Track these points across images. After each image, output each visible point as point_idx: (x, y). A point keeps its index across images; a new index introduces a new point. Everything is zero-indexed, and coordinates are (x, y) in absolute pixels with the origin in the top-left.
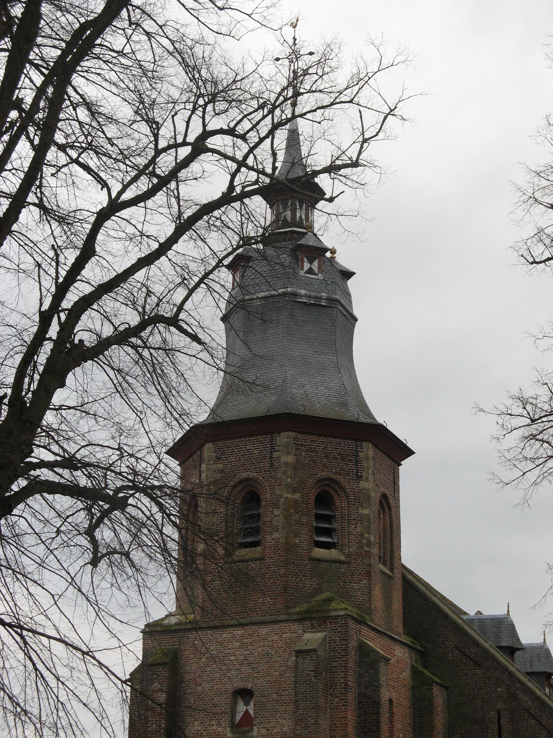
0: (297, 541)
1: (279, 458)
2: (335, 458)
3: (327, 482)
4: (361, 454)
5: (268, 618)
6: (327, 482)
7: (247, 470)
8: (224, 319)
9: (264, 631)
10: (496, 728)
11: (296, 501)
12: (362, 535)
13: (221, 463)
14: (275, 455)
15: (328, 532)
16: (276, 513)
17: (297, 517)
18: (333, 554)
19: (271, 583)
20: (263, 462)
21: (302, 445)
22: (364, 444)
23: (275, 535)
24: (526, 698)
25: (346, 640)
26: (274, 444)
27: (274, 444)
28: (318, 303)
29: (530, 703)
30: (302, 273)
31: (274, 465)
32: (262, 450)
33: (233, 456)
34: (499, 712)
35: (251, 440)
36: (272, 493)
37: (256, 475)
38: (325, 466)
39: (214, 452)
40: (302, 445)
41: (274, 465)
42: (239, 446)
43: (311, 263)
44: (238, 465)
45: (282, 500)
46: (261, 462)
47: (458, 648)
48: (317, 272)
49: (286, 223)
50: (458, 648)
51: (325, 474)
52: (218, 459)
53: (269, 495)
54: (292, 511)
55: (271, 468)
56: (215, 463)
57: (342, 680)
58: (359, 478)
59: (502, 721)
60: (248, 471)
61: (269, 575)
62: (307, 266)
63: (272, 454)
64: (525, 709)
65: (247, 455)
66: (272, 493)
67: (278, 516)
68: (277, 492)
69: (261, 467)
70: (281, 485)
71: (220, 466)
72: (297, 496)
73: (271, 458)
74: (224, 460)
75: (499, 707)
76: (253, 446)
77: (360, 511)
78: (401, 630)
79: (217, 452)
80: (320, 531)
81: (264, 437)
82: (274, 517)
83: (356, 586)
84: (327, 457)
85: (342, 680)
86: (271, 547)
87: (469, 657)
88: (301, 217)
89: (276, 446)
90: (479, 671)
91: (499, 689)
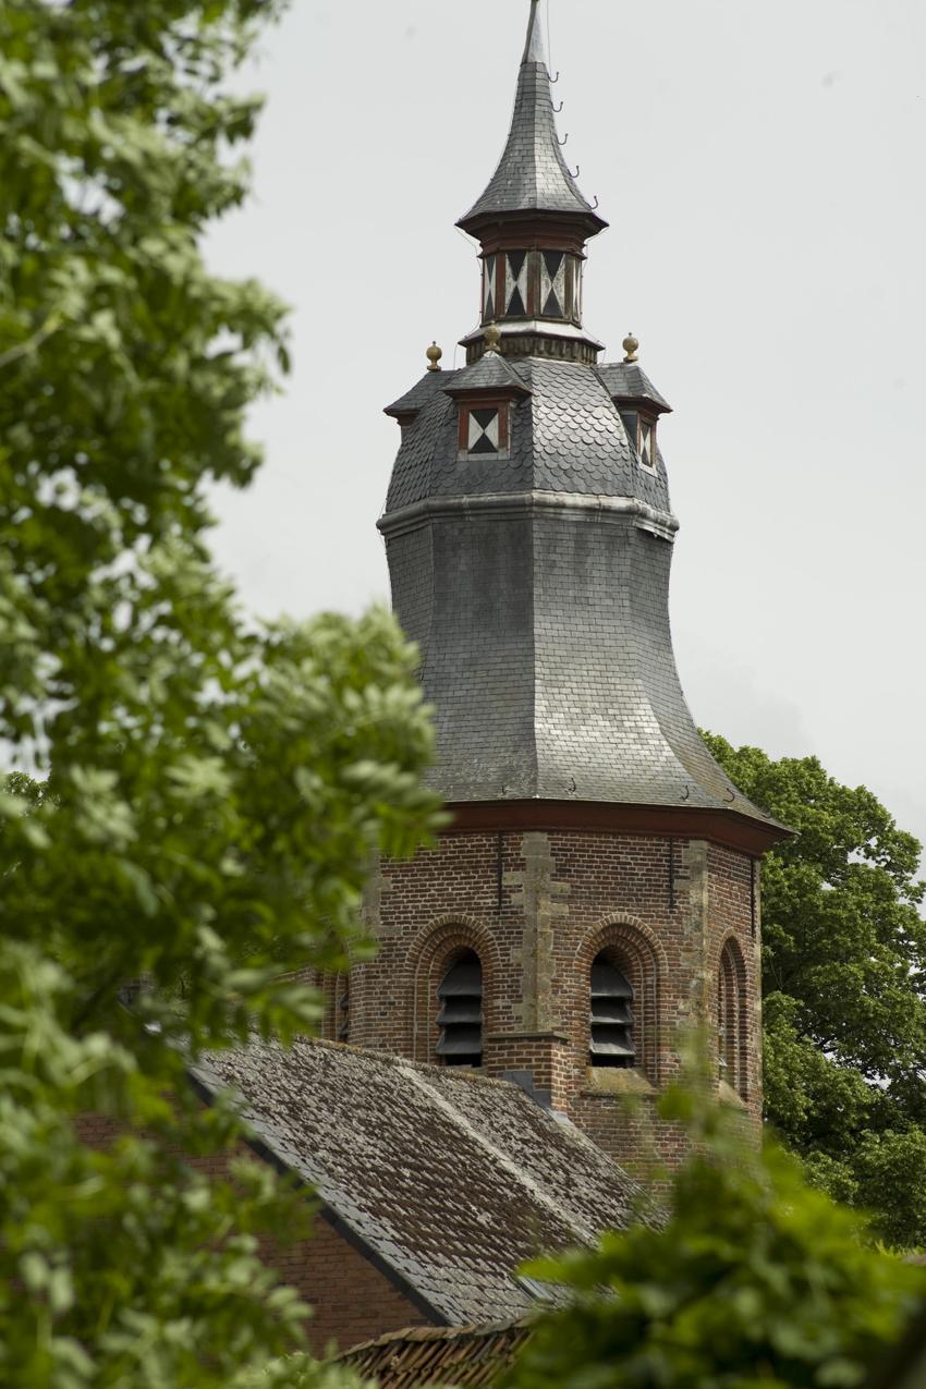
13: (568, 881)
16: (681, 1007)
19: (676, 1150)
20: (655, 896)
26: (676, 861)
27: (676, 861)
31: (676, 907)
32: (651, 870)
33: (593, 872)
35: (629, 843)
36: (674, 965)
37: (640, 920)
39: (553, 855)
41: (676, 907)
42: (605, 852)
44: (602, 893)
45: (694, 982)
46: (650, 895)
49: (516, 312)
53: (667, 967)
55: (671, 912)
56: (554, 877)
60: (623, 910)
61: (671, 1134)
63: (671, 881)
65: (620, 874)
66: (674, 965)
67: (687, 1014)
68: (685, 965)
69: (650, 906)
70: (690, 951)
71: (567, 886)
74: (573, 876)
79: (557, 855)
81: (655, 842)
86: (673, 1077)
88: (516, 291)
89: (680, 867)
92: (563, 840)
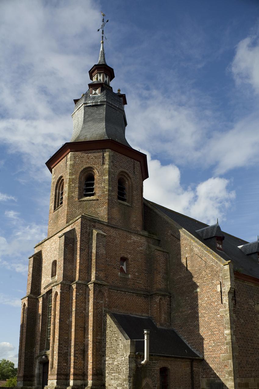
0: (73, 195)
2: (92, 158)
6: (89, 169)
11: (73, 179)
12: (104, 187)
17: (73, 185)
18: (92, 198)
22: (107, 150)
24: (196, 249)
28: (96, 104)
29: (198, 251)
34: (186, 258)
38: (87, 162)
40: (77, 156)
43: (95, 91)
48: (98, 94)
51: (87, 166)
54: (71, 183)
59: (187, 262)
62: (94, 92)
72: (74, 177)
75: (186, 256)
77: (104, 178)
84: (88, 159)
87: (175, 237)
91: (187, 248)
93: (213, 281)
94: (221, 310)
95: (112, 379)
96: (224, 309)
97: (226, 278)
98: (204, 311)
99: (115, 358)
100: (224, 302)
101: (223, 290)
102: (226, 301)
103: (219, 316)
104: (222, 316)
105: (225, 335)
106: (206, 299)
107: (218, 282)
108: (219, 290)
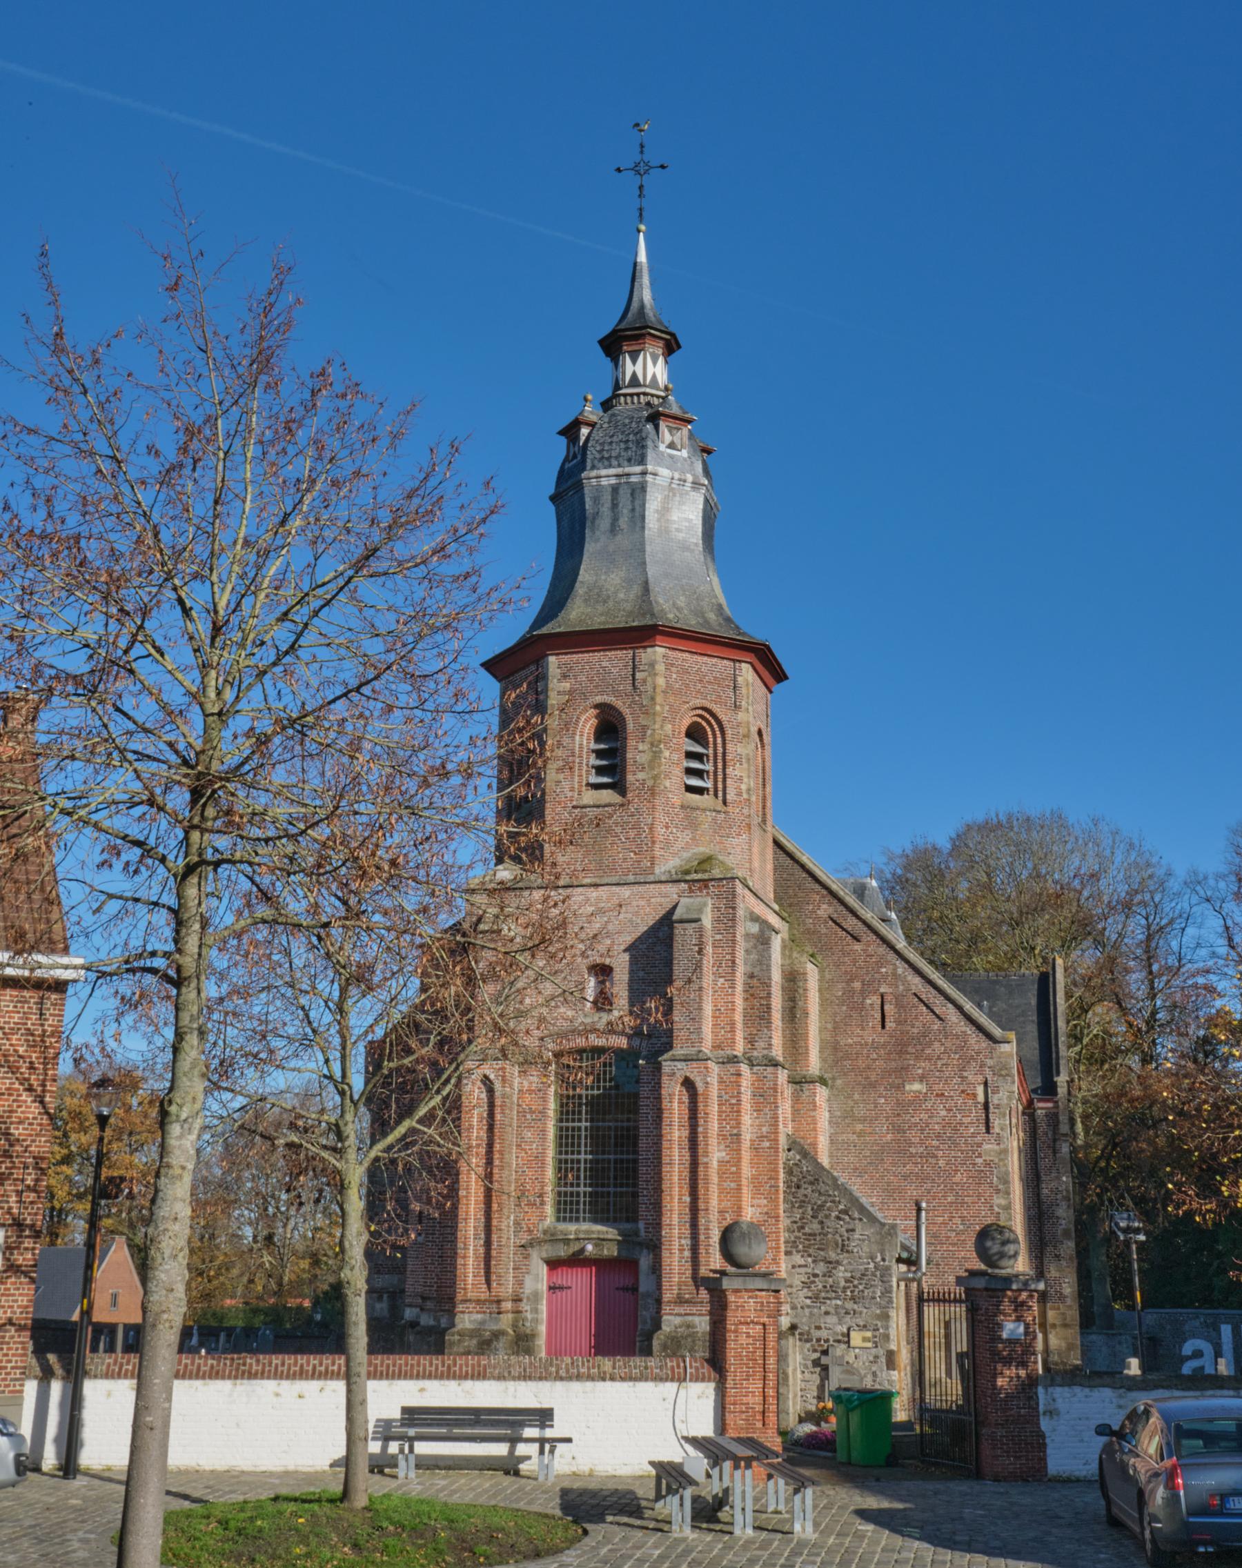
1: (644, 681)
3: (700, 712)
4: (739, 679)
5: (631, 878)
6: (700, 712)
7: (602, 693)
8: (553, 499)
9: (625, 892)
10: (878, 1016)
12: (741, 779)
14: (638, 675)
15: (698, 773)
16: (641, 748)
21: (672, 665)
23: (641, 776)
25: (734, 908)
30: (662, 447)
40: (672, 665)
47: (832, 919)
50: (832, 919)
52: (565, 676)
57: (728, 957)
58: (737, 707)
59: (886, 1007)
64: (915, 994)
68: (644, 723)
73: (634, 679)
75: (882, 990)
76: (612, 661)
78: (772, 896)
80: (690, 772)
82: (637, 752)
83: (735, 841)
85: (728, 957)
90: (858, 947)
91: (884, 970)
92: (565, 658)
93: (965, 1074)
94: (986, 1146)
95: (827, 1313)
96: (996, 1147)
97: (1003, 1073)
98: (935, 1143)
99: (838, 1263)
100: (997, 1130)
101: (994, 1099)
102: (1002, 1129)
103: (979, 1161)
104: (987, 1164)
105: (996, 1209)
106: (944, 1113)
107: (980, 1078)
108: (981, 1098)
